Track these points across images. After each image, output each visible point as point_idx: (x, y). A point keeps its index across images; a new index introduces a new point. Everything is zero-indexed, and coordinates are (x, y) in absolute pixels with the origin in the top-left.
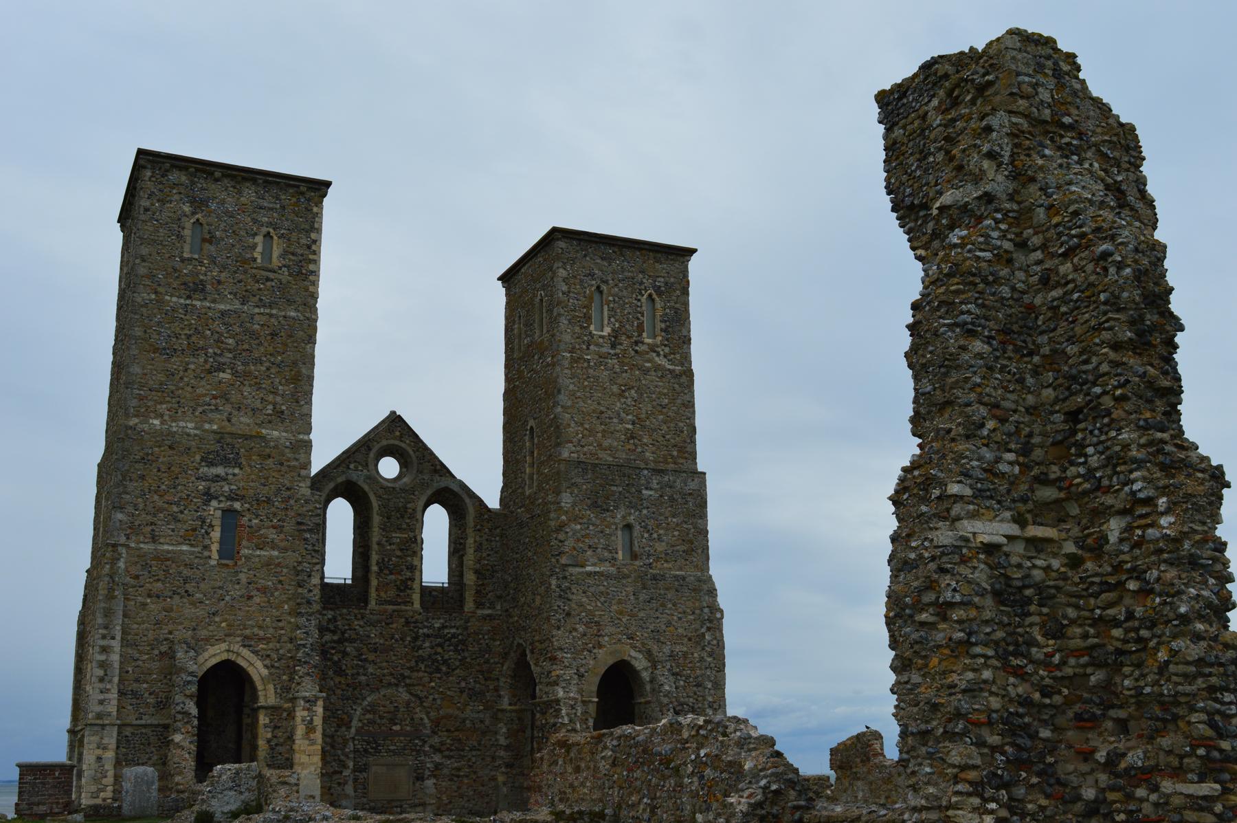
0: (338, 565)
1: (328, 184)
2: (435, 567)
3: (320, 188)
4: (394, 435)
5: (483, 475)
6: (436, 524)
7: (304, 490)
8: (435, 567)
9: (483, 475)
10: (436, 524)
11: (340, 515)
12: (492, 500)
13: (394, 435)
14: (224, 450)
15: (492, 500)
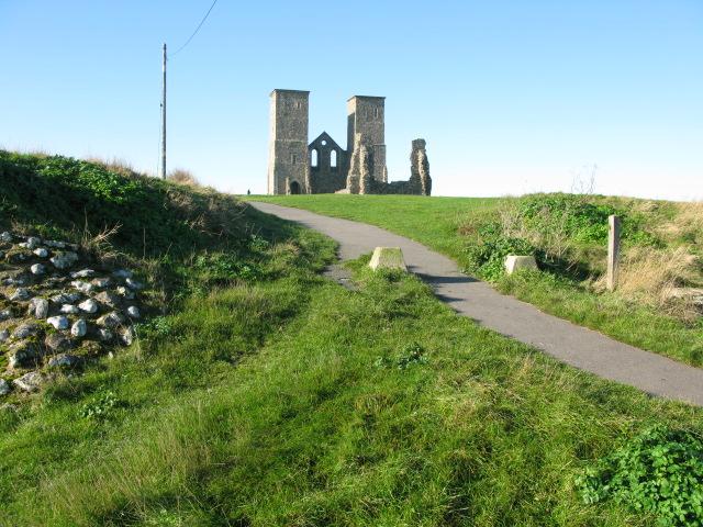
0: (314, 163)
1: (308, 92)
2: (333, 163)
3: (308, 92)
4: (324, 136)
5: (344, 146)
6: (333, 154)
7: (306, 151)
8: (333, 163)
9: (344, 146)
10: (333, 154)
11: (314, 153)
12: (345, 148)
13: (324, 136)
14: (293, 145)
15: (345, 148)
